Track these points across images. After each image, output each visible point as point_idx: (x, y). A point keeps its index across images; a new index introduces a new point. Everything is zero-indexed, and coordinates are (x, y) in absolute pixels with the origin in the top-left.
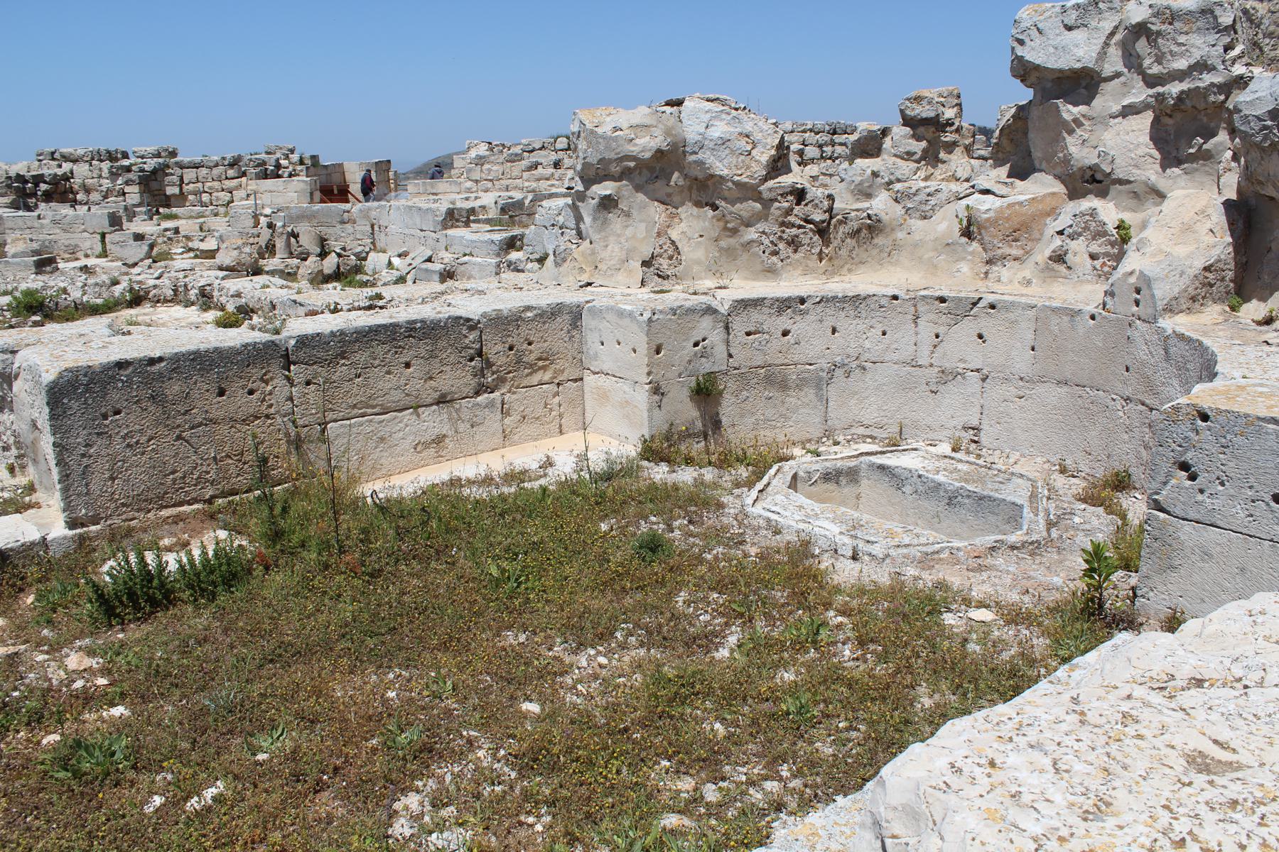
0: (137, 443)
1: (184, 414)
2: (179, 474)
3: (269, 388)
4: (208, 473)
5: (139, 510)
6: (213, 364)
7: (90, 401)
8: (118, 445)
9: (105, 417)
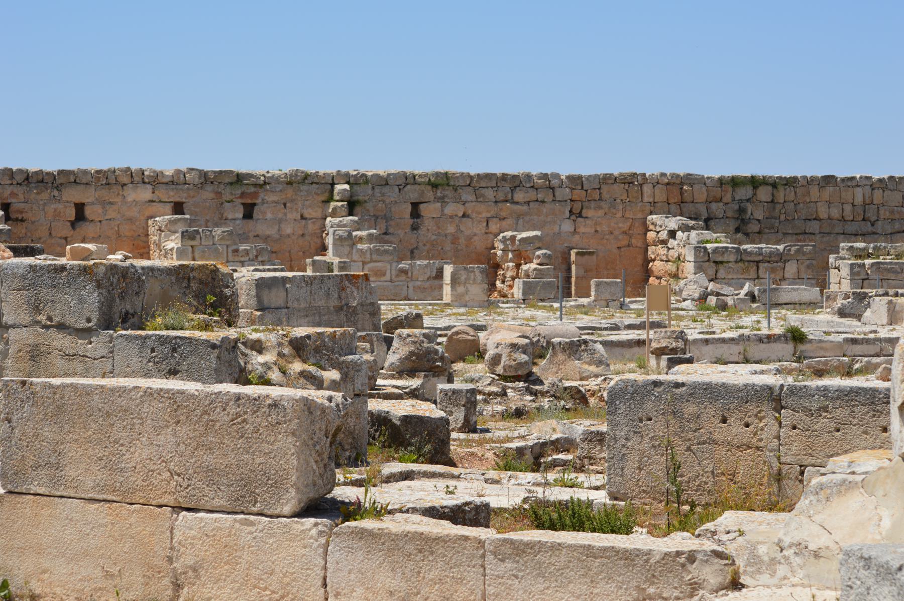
0: (659, 445)
1: (695, 431)
2: (685, 479)
3: (762, 424)
4: (706, 483)
5: (654, 499)
6: (720, 396)
7: (632, 406)
8: (646, 444)
9: (641, 420)
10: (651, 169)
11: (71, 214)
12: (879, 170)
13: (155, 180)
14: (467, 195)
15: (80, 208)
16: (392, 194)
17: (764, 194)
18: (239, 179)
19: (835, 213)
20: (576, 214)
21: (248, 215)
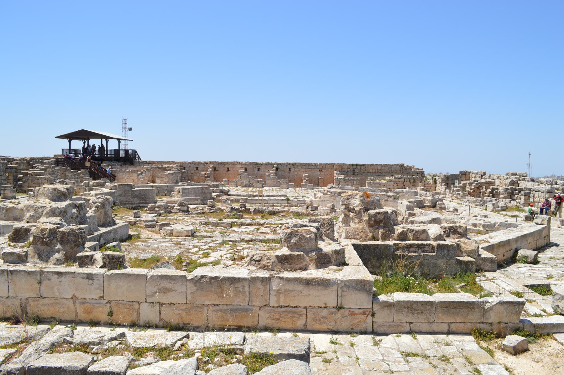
10: (336, 162)
11: (227, 169)
12: (383, 163)
13: (242, 164)
14: (299, 167)
15: (228, 168)
16: (285, 167)
17: (359, 167)
18: (257, 164)
19: (374, 171)
20: (321, 171)
21: (259, 170)
